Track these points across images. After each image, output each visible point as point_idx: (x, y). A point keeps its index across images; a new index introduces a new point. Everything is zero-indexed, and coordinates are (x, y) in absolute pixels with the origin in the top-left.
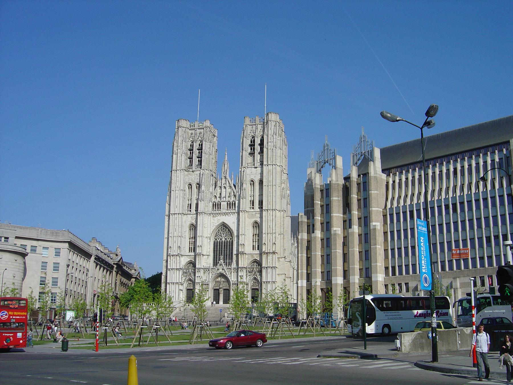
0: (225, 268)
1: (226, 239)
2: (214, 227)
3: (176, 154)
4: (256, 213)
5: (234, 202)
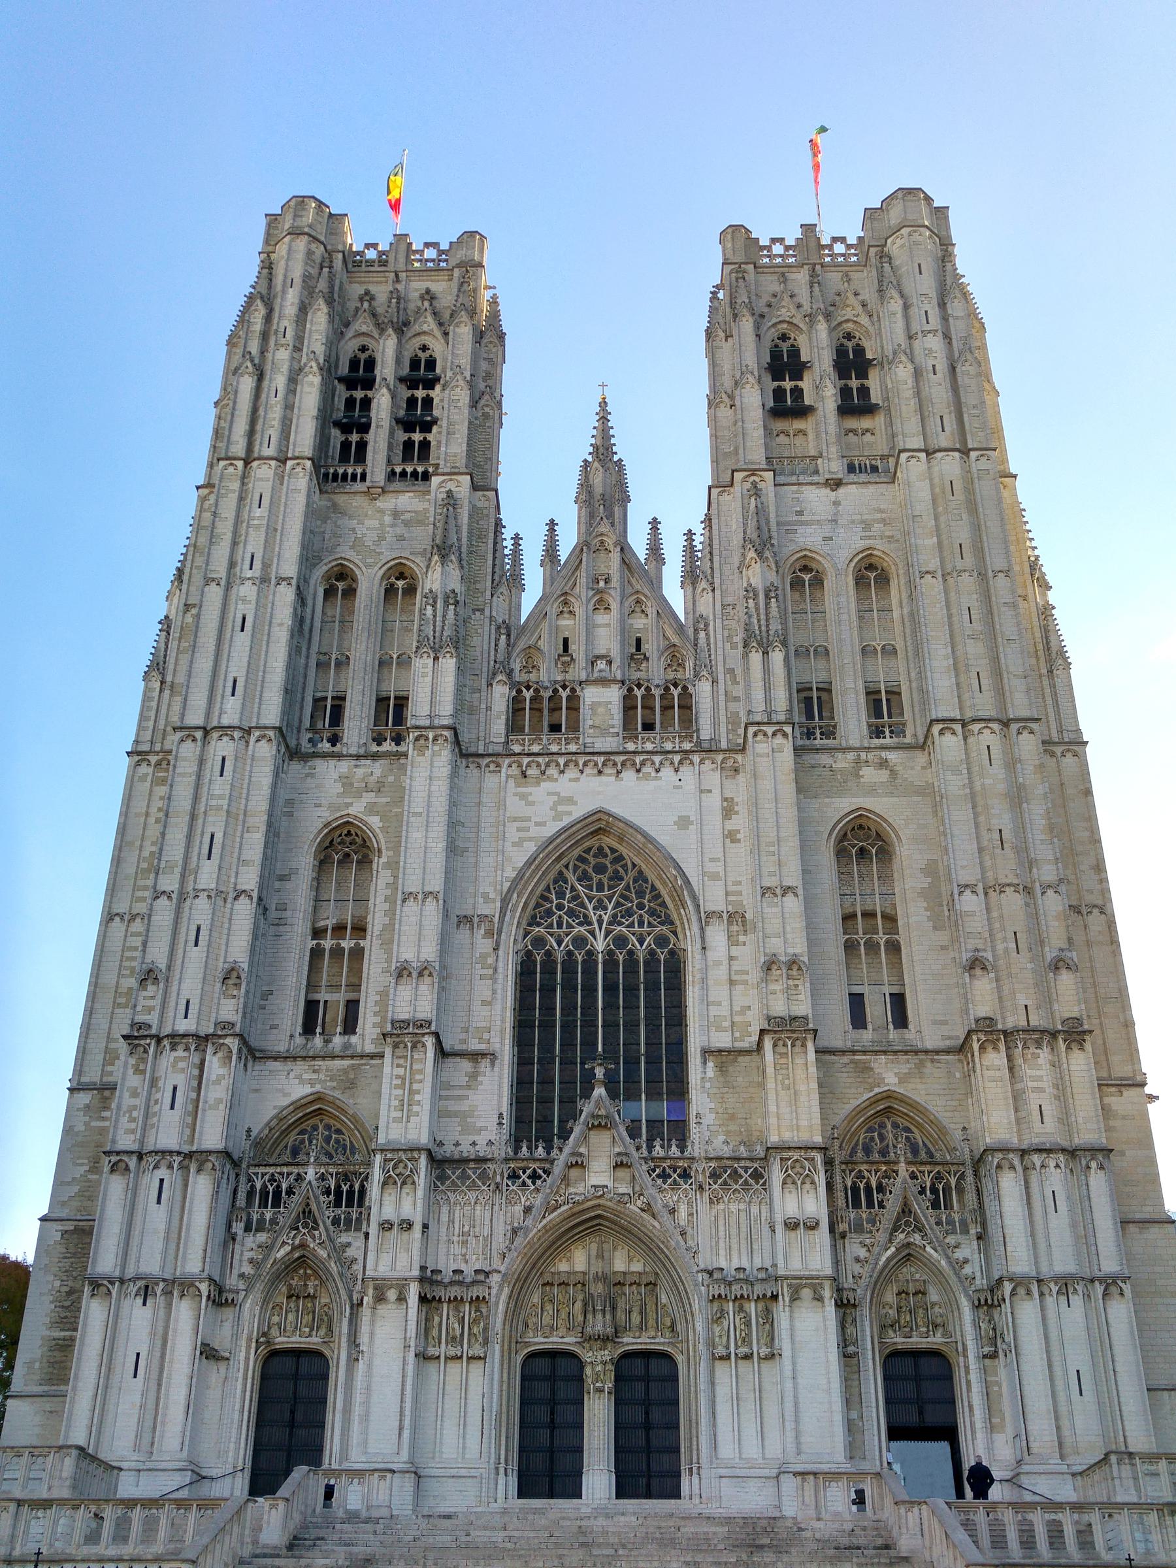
1: (621, 941)
2: (531, 848)
4: (857, 762)
5: (676, 692)
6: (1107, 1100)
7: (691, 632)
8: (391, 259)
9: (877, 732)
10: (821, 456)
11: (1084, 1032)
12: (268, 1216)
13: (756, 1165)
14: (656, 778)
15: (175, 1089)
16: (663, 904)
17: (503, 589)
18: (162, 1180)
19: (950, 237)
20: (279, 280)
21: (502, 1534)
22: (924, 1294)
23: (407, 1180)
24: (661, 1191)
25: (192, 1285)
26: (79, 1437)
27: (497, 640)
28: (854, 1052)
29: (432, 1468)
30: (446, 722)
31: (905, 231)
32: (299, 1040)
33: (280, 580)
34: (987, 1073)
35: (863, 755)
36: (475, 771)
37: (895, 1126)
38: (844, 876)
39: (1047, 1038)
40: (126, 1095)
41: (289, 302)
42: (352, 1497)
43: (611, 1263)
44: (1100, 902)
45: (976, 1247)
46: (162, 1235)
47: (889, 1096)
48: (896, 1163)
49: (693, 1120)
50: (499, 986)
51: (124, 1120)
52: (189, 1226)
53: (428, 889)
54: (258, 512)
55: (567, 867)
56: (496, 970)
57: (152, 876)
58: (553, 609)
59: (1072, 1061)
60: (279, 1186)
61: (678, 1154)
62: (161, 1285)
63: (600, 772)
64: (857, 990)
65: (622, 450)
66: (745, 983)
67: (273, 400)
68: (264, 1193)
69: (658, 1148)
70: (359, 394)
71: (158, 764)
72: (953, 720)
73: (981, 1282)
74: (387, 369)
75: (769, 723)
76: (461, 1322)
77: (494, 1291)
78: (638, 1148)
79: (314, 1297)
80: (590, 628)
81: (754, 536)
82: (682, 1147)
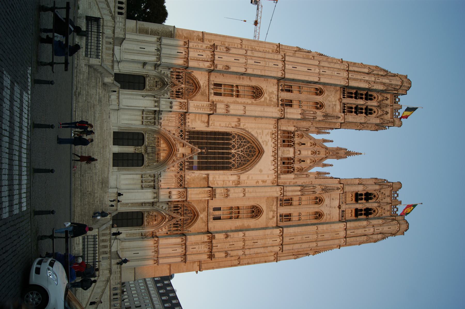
0: (186, 158)
1: (234, 156)
2: (256, 135)
3: (369, 71)
4: (274, 211)
6: (197, 262)
7: (306, 173)
8: (396, 104)
9: (281, 216)
10: (346, 204)
11: (211, 258)
12: (174, 76)
13: (183, 185)
14: (271, 165)
15: (203, 55)
16: (242, 166)
17: (317, 130)
18: (182, 53)
19: (397, 235)
20: (391, 78)
21: (106, 129)
22: (155, 221)
23: (181, 108)
24: (178, 164)
25: (159, 60)
26: (127, 36)
27: (305, 128)
28: (208, 208)
29: (120, 112)
30: (286, 116)
31: (399, 225)
32: (213, 83)
33: (320, 78)
34: (203, 237)
35: (276, 212)
36: (274, 123)
37: (191, 216)
38: (248, 208)
39: (210, 250)
40: (201, 45)
41: (386, 81)
42: (114, 96)
43: (162, 153)
44: (241, 263)
45: (165, 232)
46: (170, 53)
47: (198, 216)
48: (183, 216)
49: (193, 171)
50: (224, 128)
51: (196, 44)
52: (172, 59)
53: (247, 112)
54: (336, 73)
55: (251, 144)
56: (228, 127)
57: (251, 49)
58: (312, 141)
59: (205, 255)
60: (180, 79)
61: (186, 168)
62: (159, 53)
63: (273, 152)
64: (222, 209)
65: (349, 158)
66: (224, 184)
67: (362, 77)
68: (179, 76)
69: (187, 163)
70: (364, 96)
71: (277, 50)
72: (283, 233)
73: (158, 234)
74: (370, 103)
75: (283, 191)
76: (150, 119)
77: (157, 127)
78: (187, 159)
79: (156, 87)
80: (307, 149)
81: (328, 189)
82: (187, 169)
